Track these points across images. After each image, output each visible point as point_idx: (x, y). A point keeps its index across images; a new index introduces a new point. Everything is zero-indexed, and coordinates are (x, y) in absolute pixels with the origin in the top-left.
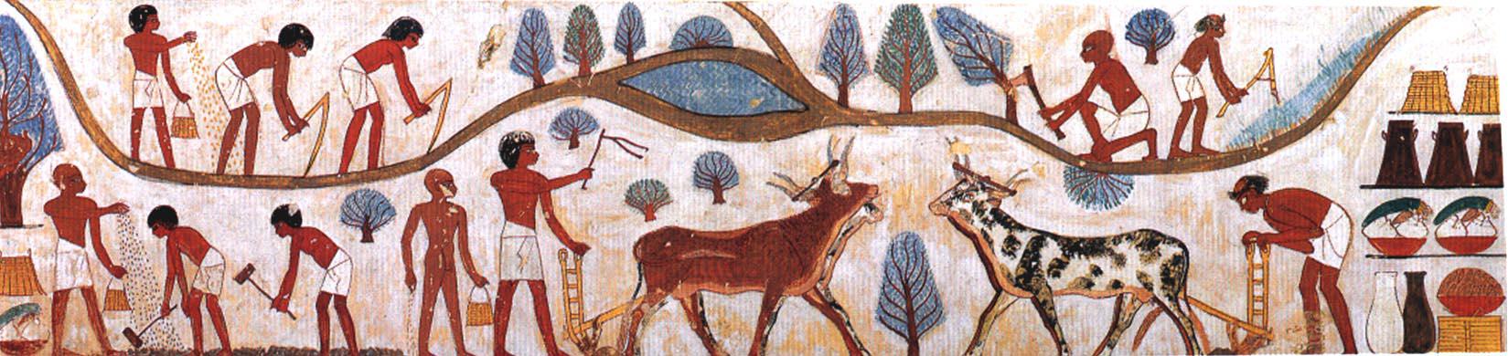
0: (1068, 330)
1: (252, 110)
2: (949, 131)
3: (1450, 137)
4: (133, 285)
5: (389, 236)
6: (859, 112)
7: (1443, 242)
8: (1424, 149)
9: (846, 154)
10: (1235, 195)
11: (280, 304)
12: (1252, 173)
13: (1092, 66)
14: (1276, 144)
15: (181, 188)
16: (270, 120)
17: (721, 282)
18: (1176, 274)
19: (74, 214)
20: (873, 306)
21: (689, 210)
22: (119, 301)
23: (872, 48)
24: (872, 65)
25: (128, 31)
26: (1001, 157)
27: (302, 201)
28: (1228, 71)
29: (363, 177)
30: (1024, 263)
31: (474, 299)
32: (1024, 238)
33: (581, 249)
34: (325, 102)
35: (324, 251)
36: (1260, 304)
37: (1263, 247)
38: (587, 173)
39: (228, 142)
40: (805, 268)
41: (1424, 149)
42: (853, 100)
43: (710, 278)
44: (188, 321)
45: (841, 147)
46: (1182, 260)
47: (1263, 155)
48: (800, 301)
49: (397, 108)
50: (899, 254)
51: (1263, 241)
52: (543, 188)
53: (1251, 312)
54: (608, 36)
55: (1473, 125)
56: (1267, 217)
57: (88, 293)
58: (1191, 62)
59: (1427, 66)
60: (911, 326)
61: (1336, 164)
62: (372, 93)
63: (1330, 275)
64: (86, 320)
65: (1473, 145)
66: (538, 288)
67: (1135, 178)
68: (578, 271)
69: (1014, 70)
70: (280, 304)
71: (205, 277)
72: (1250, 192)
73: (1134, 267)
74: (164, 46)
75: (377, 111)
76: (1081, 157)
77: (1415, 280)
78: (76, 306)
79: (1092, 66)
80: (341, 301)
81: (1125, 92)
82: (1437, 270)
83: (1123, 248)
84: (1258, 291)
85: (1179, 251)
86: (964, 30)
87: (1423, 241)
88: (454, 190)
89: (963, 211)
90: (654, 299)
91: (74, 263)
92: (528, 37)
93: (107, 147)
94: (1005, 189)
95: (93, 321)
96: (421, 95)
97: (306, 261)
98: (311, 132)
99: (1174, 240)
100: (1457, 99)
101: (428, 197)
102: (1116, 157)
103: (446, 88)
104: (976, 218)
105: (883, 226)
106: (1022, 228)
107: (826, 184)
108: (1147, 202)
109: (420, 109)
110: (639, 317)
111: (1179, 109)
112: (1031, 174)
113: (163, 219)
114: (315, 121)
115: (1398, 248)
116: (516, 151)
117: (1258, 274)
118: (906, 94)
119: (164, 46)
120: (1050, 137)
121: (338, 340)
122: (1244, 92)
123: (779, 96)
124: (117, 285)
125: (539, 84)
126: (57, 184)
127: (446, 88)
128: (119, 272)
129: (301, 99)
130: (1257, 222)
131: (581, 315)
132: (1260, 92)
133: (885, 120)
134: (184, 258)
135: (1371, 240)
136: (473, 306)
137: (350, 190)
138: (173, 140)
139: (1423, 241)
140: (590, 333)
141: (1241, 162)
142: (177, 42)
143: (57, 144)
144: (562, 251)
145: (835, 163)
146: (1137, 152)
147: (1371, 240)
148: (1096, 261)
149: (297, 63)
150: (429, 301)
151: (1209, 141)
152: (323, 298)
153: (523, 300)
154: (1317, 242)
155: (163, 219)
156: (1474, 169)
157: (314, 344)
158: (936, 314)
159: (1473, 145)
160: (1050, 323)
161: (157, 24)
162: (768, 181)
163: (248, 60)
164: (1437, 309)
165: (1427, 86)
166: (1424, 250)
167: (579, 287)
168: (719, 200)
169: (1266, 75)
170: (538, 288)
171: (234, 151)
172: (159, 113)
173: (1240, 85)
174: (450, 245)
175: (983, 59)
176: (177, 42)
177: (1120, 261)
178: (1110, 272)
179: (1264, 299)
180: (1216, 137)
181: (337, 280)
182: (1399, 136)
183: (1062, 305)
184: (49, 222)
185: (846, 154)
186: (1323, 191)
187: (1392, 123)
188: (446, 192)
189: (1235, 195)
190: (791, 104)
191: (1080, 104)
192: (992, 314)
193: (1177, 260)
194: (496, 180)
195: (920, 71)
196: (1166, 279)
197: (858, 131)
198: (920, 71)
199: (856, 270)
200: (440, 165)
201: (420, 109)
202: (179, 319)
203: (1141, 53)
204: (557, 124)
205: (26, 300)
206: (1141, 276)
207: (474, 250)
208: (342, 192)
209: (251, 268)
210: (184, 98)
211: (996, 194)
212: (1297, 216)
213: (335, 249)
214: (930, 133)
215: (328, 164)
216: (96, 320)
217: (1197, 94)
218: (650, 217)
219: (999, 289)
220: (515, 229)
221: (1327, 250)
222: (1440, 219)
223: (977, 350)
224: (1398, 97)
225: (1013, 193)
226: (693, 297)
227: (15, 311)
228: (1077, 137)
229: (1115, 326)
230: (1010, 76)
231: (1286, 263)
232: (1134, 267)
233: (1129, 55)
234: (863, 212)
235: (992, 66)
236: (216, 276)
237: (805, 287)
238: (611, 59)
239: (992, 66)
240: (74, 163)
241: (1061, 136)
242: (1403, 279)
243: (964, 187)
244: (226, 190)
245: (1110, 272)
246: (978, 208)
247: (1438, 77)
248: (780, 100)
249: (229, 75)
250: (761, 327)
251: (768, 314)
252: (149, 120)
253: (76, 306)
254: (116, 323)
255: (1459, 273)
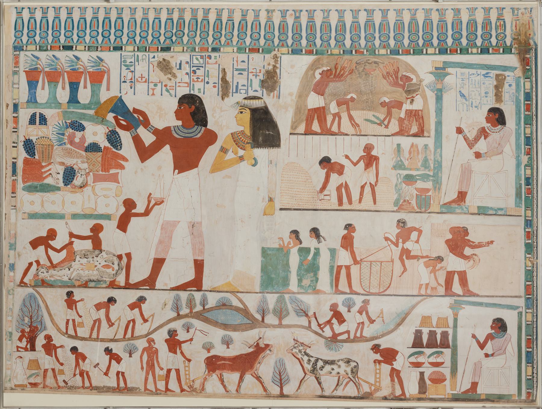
0: (324, 385)
1: (99, 320)
2: (293, 330)
3: (432, 334)
4: (65, 368)
5: (136, 356)
6: (267, 324)
7: (431, 364)
8: (425, 339)
9: (263, 336)
10: (372, 349)
11: (106, 374)
12: (377, 343)
13: (332, 313)
14: (383, 335)
15: (80, 341)
16: (104, 323)
17: (228, 370)
18: (355, 371)
19: (50, 348)
20: (270, 378)
21: (220, 350)
22: (62, 372)
23: (271, 307)
24: (271, 311)
25: (66, 298)
26: (307, 337)
27: (111, 345)
28: (370, 314)
29: (129, 339)
30: (313, 367)
31: (160, 374)
32: (313, 360)
33: (189, 360)
34: (119, 319)
35: (118, 360)
36: (378, 380)
37: (379, 364)
38: (191, 340)
39: (92, 329)
40: (252, 367)
41: (425, 339)
42: (266, 321)
43: (225, 369)
44: (81, 378)
45: (262, 334)
46: (357, 367)
47: (380, 338)
48: (250, 376)
49: (139, 320)
50: (278, 364)
51: (380, 362)
52: (180, 343)
53: (376, 382)
54: (198, 302)
55: (439, 331)
56: (381, 356)
57: (53, 370)
58: (360, 312)
59: (426, 315)
60: (281, 384)
61: (401, 340)
62: (132, 315)
63: (398, 372)
64: (53, 378)
65: (439, 337)
66: (178, 371)
67: (344, 344)
68: (189, 367)
69: (311, 313)
70: (106, 374)
71: (85, 366)
72: (376, 348)
73: (344, 368)
74: (75, 302)
75: (134, 321)
76: (329, 338)
77: (422, 374)
78: (50, 374)
79: (332, 313)
80: (123, 373)
81: (341, 320)
82: (428, 371)
83: (341, 363)
84: (378, 376)
85: (356, 364)
86: (297, 302)
87: (424, 363)
88: (155, 343)
89: (296, 352)
90: (209, 374)
91: (49, 362)
92: (175, 302)
93: (59, 330)
94: (308, 346)
95: (54, 378)
96: (146, 317)
97: (113, 362)
98: (115, 327)
99: (355, 361)
100: (434, 323)
101: (147, 345)
102: (339, 338)
103: (153, 315)
104: (299, 354)
105: (273, 356)
106: (312, 357)
107: (258, 344)
108: (346, 350)
109: (145, 321)
110: (205, 379)
111: (356, 325)
112: (314, 342)
113: (74, 350)
114: (116, 324)
115: (418, 365)
116: (172, 333)
117: (378, 371)
118: (280, 319)
119: (75, 302)
120: (320, 331)
121: (122, 384)
122: (375, 321)
123: (245, 319)
124: (61, 368)
125: (179, 315)
126: (45, 339)
127: (153, 315)
128: (62, 364)
129: (113, 317)
130: (378, 357)
131: (189, 379)
132: (378, 320)
133: (274, 326)
134: (80, 361)
135: (410, 363)
136: (159, 376)
137: (125, 343)
138: (77, 328)
139: (424, 363)
140: (192, 384)
141: (373, 340)
142: (79, 301)
143: (45, 328)
144: (184, 361)
145: (260, 338)
146: (345, 337)
147: (410, 363)
148: (333, 366)
149: (112, 307)
150: (147, 373)
151: (364, 334)
152: (118, 373)
153: (173, 374)
154: (394, 363)
155: (74, 350)
156: (439, 343)
157: (116, 386)
158: (288, 380)
159: (439, 337)
160: (320, 383)
161: (73, 296)
162: (241, 343)
163: (98, 307)
164: (428, 382)
165: (426, 320)
166: (424, 366)
167: (189, 371)
168: (228, 348)
169: (381, 316)
170: (178, 371)
171: (94, 331)
172: (74, 321)
173: (373, 319)
174: (153, 359)
175: (302, 310)
176: (79, 301)
177: (339, 366)
178: (337, 370)
179: (379, 378)
180: (368, 332)
181: (122, 367)
182: (418, 334)
183: (322, 379)
184: (43, 350)
185: (263, 336)
186: (396, 348)
187: (416, 330)
188: (152, 344)
189: (372, 349)
190: (249, 322)
191: (329, 322)
192: (303, 381)
193: (355, 367)
194: (166, 341)
195: (284, 313)
196: (352, 372)
197: (267, 329)
198: (284, 313)
199: (266, 367)
200: (150, 336)
201: (145, 321)
202: (78, 377)
203: (346, 309)
204: (183, 326)
205: (36, 371)
206: (345, 371)
207: (160, 360)
208: (124, 343)
209: (98, 364)
210: (81, 317)
211: (305, 347)
212: (389, 356)
213: (122, 359)
214: (287, 330)
215: (120, 336)
216: (55, 377)
217: (362, 321)
218: (209, 351)
219: (306, 374)
220: (171, 354)
221: (397, 365)
222: (429, 357)
223: (299, 391)
224: (418, 322)
225: (310, 347)
226: (221, 374)
227: (33, 374)
228: (328, 332)
229: (338, 385)
230: (309, 315)
231: (386, 368)
232: (344, 368)
233: (342, 309)
234: (268, 352)
235: (305, 312)
236: (88, 366)
237: (252, 372)
238: (199, 308)
239: (305, 312)
240: (50, 334)
241: (323, 332)
242: (419, 374)
243: (296, 345)
244: (92, 342)
245: (337, 370)
246: (300, 351)
247: (429, 317)
248: (246, 321)
249: (93, 310)
250: (239, 383)
251: (241, 379)
252: (71, 322)
253: (50, 374)
254: (60, 378)
255: (434, 372)
